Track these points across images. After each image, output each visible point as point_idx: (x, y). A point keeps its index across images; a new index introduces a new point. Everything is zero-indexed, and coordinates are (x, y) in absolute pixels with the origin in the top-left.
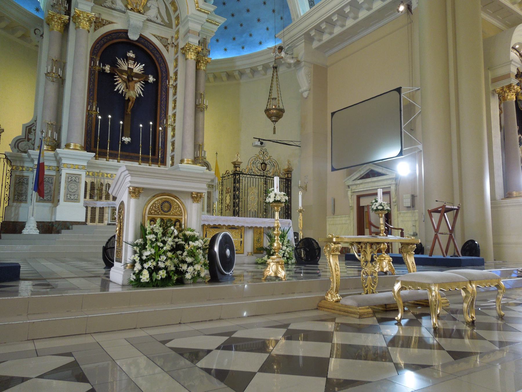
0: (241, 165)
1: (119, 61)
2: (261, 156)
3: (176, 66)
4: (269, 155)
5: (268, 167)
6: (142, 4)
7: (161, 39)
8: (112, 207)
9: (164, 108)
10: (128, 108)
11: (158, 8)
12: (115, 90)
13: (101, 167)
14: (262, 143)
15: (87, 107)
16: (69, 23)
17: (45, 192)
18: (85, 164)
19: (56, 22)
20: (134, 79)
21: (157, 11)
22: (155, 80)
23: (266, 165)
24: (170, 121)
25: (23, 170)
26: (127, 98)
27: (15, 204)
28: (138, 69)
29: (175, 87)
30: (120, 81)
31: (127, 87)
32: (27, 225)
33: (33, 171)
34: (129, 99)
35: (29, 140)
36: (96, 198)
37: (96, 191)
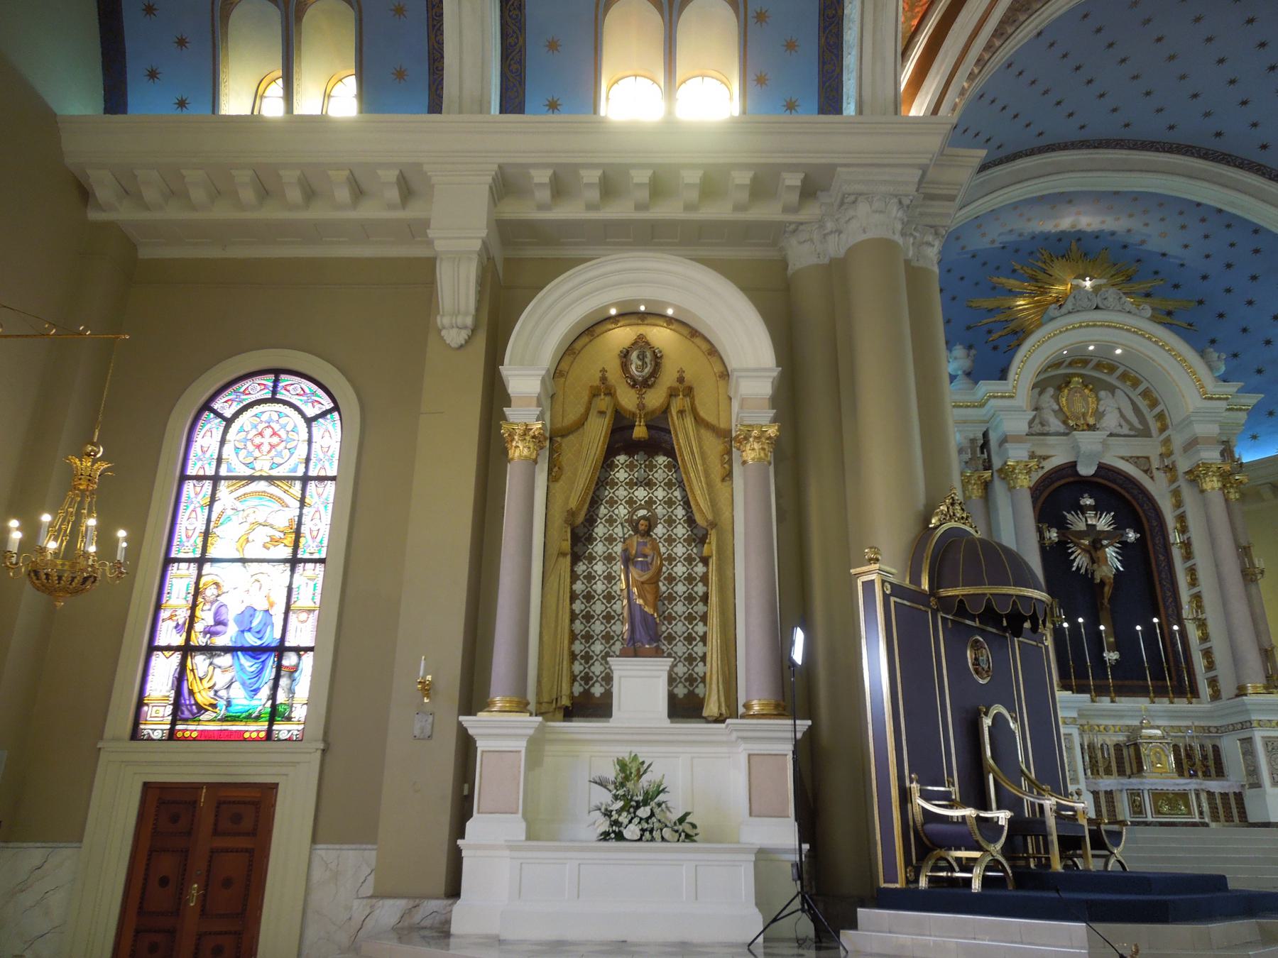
1: (1069, 516)
3: (1179, 504)
6: (1090, 411)
7: (1135, 460)
8: (1127, 790)
9: (1168, 585)
10: (1103, 599)
11: (1119, 409)
12: (1074, 569)
13: (1087, 715)
16: (992, 481)
18: (1075, 715)
19: (975, 484)
20: (1105, 542)
21: (1119, 415)
22: (1139, 535)
28: (1103, 523)
30: (1079, 551)
31: (1093, 561)
34: (1101, 580)
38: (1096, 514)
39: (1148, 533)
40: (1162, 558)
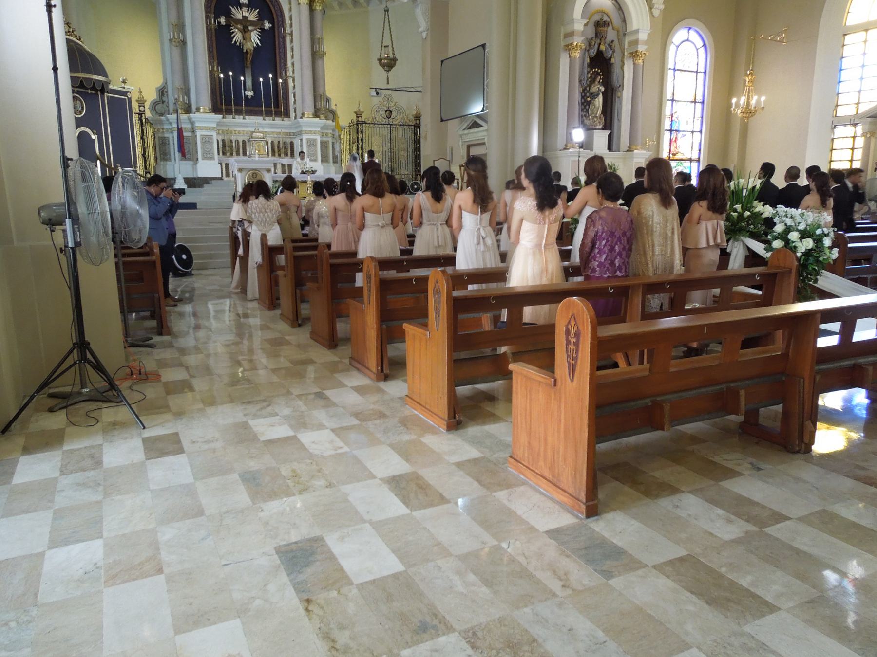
0: (363, 115)
2: (386, 103)
4: (395, 100)
5: (394, 115)
12: (233, 42)
14: (377, 94)
15: (209, 68)
17: (186, 151)
23: (391, 112)
24: (290, 73)
25: (163, 132)
26: (245, 51)
27: (162, 163)
28: (253, 16)
29: (291, 34)
32: (177, 181)
33: (172, 132)
35: (163, 102)
36: (228, 154)
37: (227, 149)
38: (248, 10)
39: (276, 24)
40: (281, 40)
